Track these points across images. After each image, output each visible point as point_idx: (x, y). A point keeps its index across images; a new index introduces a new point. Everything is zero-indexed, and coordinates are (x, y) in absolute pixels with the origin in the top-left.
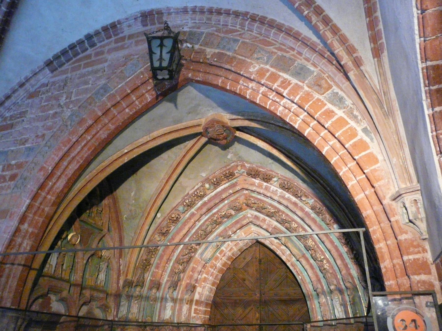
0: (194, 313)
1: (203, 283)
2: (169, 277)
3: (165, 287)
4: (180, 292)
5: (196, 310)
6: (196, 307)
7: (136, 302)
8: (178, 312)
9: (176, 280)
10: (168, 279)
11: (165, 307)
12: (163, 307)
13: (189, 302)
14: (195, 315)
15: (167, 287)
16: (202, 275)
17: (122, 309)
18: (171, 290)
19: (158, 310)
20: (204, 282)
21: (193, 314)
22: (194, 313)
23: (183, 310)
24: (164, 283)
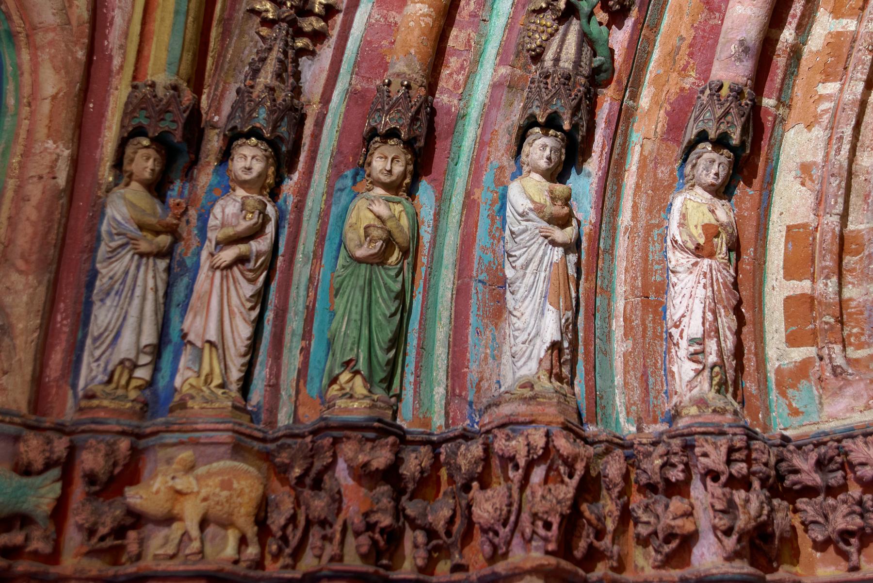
0: (793, 340)
1: (832, 88)
2: (502, 58)
3: (482, 144)
4: (630, 179)
5: (800, 308)
6: (804, 286)
7: (228, 254)
8: (628, 331)
9: (566, 64)
10: (504, 70)
11: (499, 285)
12: (478, 294)
13: (721, 244)
14: (798, 354)
15: (504, 141)
16: (804, 27)
17: (103, 316)
18: (541, 149)
19: (441, 332)
20: (828, 77)
21: (779, 352)
22: (793, 340)
23: (675, 311)
24: (474, 112)
